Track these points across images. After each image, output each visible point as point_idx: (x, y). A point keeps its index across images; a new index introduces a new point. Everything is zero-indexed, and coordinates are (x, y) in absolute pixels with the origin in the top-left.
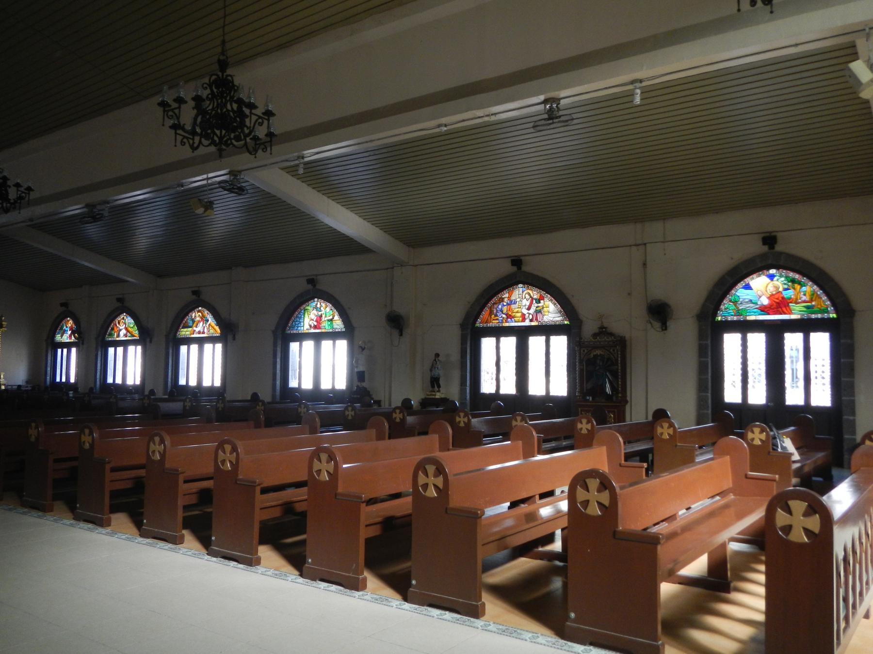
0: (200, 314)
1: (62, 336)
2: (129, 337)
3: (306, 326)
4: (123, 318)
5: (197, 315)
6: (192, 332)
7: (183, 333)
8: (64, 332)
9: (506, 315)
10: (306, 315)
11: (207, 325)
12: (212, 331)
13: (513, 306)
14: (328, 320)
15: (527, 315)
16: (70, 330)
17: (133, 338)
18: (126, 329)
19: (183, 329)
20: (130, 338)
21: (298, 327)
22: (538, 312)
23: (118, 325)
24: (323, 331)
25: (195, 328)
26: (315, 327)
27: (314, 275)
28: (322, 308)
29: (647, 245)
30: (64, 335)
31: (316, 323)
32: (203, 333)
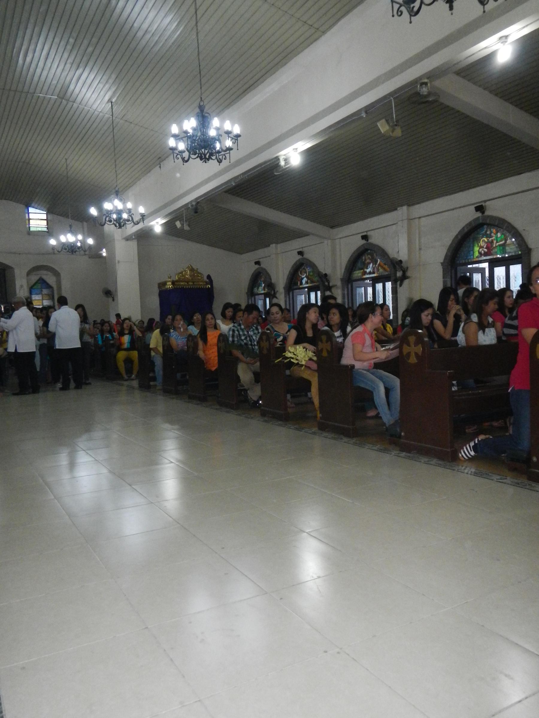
0: (369, 256)
1: (258, 289)
2: (310, 283)
3: (476, 254)
4: (304, 269)
5: (367, 257)
8: (260, 285)
11: (377, 266)
12: (381, 270)
14: (500, 245)
18: (306, 277)
21: (467, 256)
23: (300, 275)
25: (366, 270)
26: (486, 254)
27: (481, 202)
28: (493, 234)
30: (260, 287)
32: (374, 273)
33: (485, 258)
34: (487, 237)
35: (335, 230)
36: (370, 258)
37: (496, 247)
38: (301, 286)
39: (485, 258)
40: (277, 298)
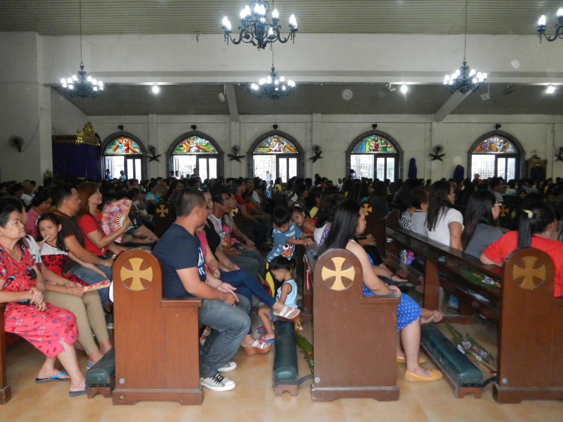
2: (201, 152)
3: (367, 149)
6: (269, 150)
7: (261, 151)
9: (489, 148)
10: (367, 144)
13: (492, 145)
14: (383, 147)
15: (499, 149)
16: (125, 146)
17: (206, 153)
18: (197, 146)
19: (259, 149)
20: (203, 153)
21: (361, 150)
22: (505, 148)
24: (380, 152)
26: (374, 150)
28: (379, 140)
29: (555, 124)
31: (374, 148)
32: (280, 151)
33: (372, 152)
34: (375, 141)
35: (241, 117)
36: (276, 140)
37: (381, 147)
38: (188, 153)
39: (372, 152)
40: (158, 161)
